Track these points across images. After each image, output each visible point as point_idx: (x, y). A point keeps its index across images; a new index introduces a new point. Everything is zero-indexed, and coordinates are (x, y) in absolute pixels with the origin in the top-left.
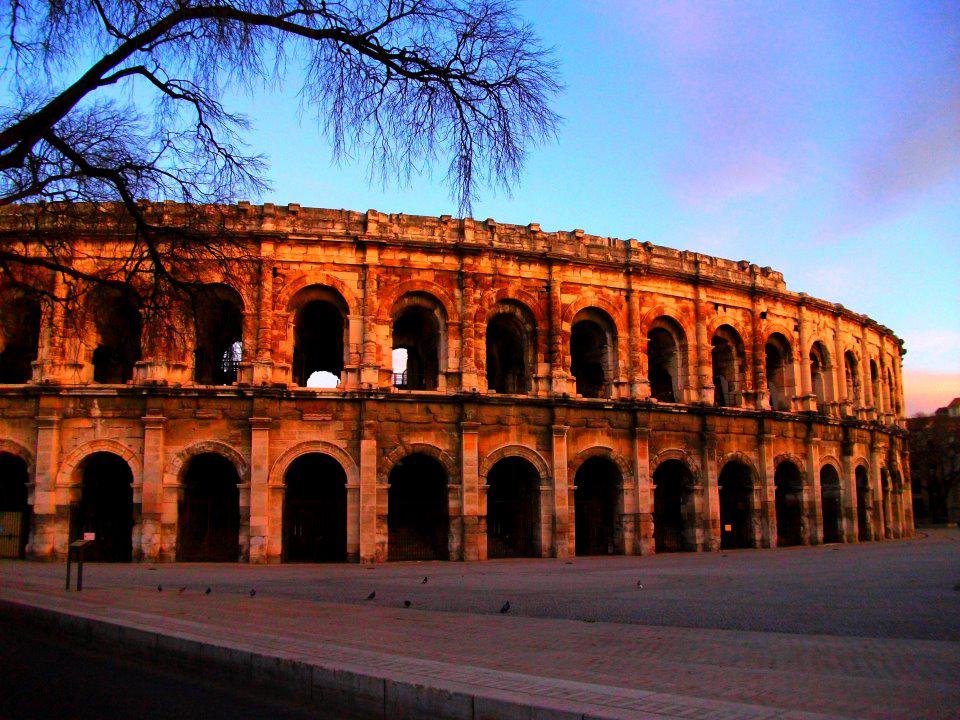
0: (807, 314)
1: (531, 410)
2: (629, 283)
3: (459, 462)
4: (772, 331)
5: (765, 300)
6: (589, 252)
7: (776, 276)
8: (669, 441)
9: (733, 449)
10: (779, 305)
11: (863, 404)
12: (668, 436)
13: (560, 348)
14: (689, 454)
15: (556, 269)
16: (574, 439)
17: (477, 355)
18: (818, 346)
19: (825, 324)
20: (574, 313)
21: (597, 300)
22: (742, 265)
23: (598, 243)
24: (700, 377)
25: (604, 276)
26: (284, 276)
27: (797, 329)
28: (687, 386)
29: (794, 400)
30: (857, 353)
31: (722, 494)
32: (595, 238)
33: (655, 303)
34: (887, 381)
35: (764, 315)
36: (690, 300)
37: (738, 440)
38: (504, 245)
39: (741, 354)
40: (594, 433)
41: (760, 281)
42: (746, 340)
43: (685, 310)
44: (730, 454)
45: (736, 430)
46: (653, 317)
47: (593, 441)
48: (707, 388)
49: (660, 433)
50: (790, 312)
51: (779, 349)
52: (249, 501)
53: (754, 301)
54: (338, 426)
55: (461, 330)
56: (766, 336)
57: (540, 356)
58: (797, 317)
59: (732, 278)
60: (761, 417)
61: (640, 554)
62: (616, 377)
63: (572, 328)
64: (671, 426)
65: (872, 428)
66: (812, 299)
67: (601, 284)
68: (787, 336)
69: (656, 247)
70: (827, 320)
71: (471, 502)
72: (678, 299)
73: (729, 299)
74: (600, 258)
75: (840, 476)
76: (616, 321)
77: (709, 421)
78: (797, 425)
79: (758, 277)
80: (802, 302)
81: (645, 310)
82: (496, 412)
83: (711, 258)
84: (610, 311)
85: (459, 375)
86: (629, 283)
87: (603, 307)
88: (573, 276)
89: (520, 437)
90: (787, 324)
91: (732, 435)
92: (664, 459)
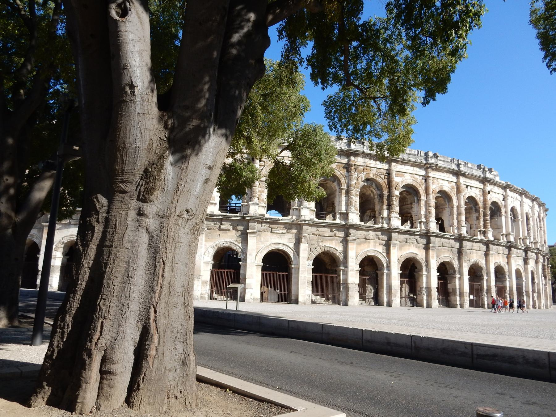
0: (509, 192)
1: (379, 233)
2: (427, 172)
3: (346, 257)
4: (492, 201)
10: (496, 187)
11: (532, 240)
13: (395, 203)
16: (400, 248)
17: (356, 205)
18: (513, 210)
19: (517, 199)
24: (459, 221)
26: (264, 162)
28: (452, 225)
31: (470, 280)
33: (438, 184)
37: (477, 253)
38: (369, 152)
39: (477, 211)
40: (410, 245)
42: (481, 204)
44: (473, 260)
47: (409, 249)
50: (501, 191)
51: (496, 210)
52: (245, 271)
53: (484, 185)
54: (290, 236)
55: (348, 192)
57: (385, 207)
58: (504, 194)
61: (431, 307)
62: (420, 219)
64: (445, 245)
68: (499, 203)
70: (517, 196)
71: (353, 277)
74: (414, 160)
77: (464, 243)
79: (487, 173)
82: (365, 233)
84: (418, 186)
85: (347, 215)
86: (427, 172)
87: (414, 184)
89: (375, 246)
92: (442, 261)
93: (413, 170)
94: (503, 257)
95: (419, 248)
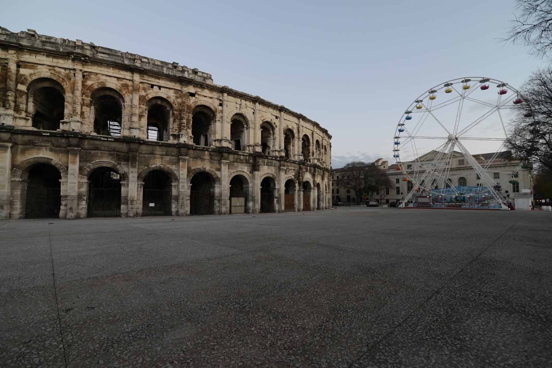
4: (199, 103)
5: (194, 86)
6: (44, 45)
7: (205, 75)
8: (101, 157)
9: (157, 163)
11: (277, 148)
12: (101, 153)
14: (120, 164)
15: (11, 52)
20: (30, 80)
21: (49, 74)
22: (175, 66)
23: (53, 41)
25: (55, 60)
27: (221, 105)
29: (215, 141)
30: (275, 123)
32: (50, 38)
34: (301, 139)
35: (193, 95)
36: (130, 80)
37: (162, 158)
39: (173, 114)
40: (40, 149)
41: (186, 75)
42: (176, 106)
43: (125, 86)
44: (153, 166)
45: (160, 153)
46: (96, 87)
47: (38, 154)
48: (133, 128)
49: (93, 152)
50: (215, 95)
56: (193, 106)
58: (221, 98)
59: (165, 71)
60: (179, 146)
63: (28, 89)
64: (103, 148)
65: (278, 159)
66: (231, 90)
67: (53, 64)
68: (212, 107)
69: (102, 48)
72: (118, 78)
73: (162, 83)
75: (249, 181)
76: (65, 87)
77: (133, 146)
78: (212, 153)
79: (186, 73)
80: (223, 90)
81: (89, 83)
83: (148, 59)
87: (55, 78)
88: (27, 57)
90: (213, 102)
91: (157, 156)
92: (97, 166)
93: (53, 62)
94: (211, 162)
95: (56, 152)
